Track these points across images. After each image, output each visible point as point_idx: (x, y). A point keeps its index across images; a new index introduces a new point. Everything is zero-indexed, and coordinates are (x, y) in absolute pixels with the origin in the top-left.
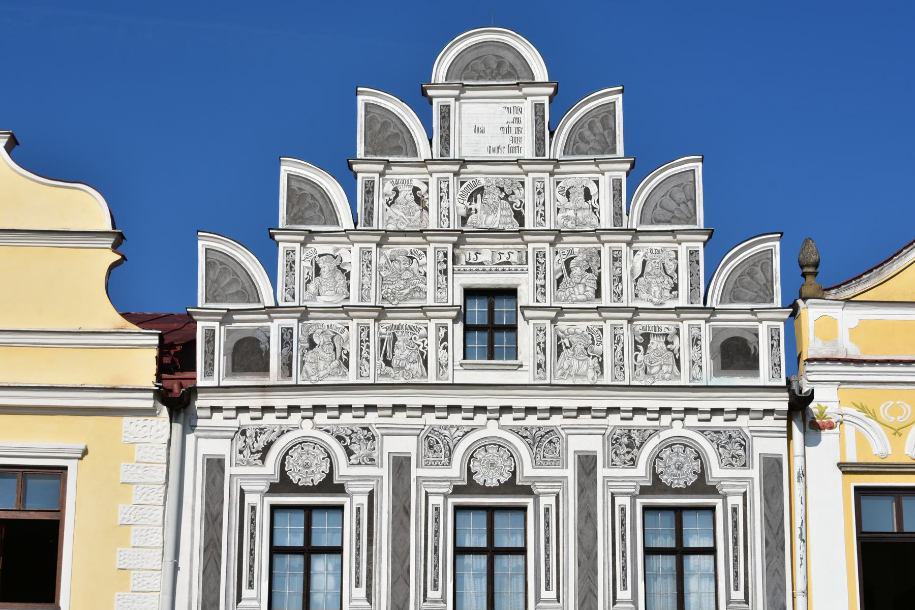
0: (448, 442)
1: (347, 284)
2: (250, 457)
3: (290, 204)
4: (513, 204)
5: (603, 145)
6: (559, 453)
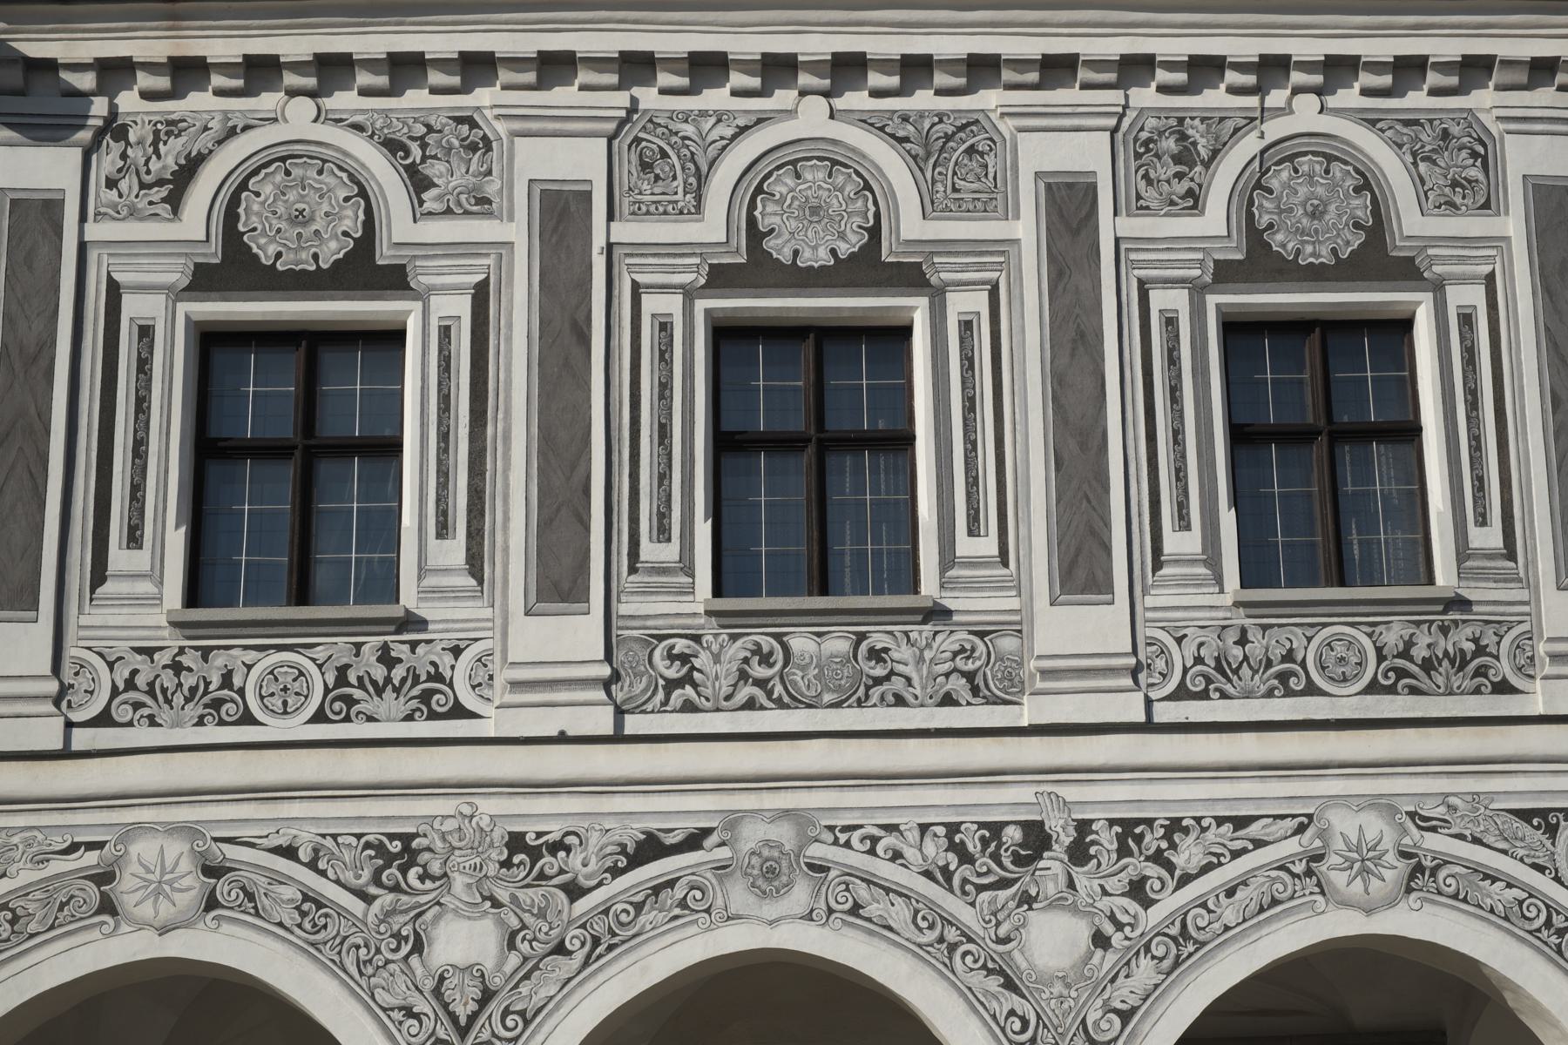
0: (692, 154)
6: (995, 178)
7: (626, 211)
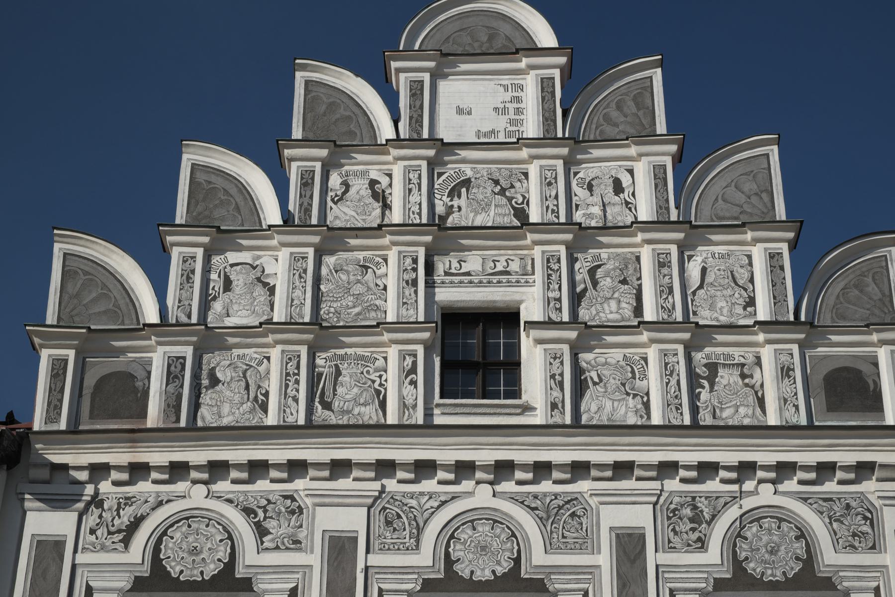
0: (415, 516)
1: (270, 301)
2: (106, 539)
3: (193, 201)
4: (512, 201)
5: (638, 127)
6: (587, 531)
7: (377, 549)
